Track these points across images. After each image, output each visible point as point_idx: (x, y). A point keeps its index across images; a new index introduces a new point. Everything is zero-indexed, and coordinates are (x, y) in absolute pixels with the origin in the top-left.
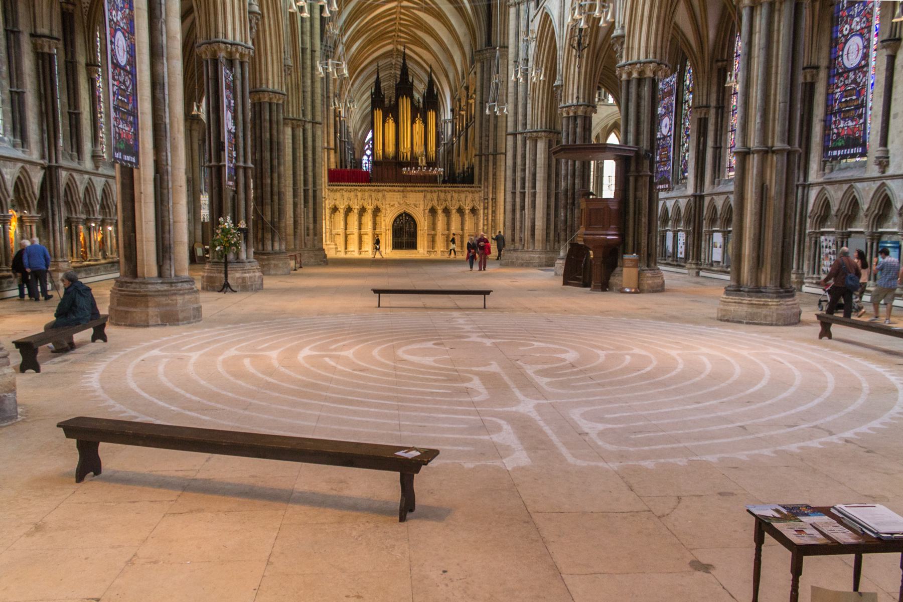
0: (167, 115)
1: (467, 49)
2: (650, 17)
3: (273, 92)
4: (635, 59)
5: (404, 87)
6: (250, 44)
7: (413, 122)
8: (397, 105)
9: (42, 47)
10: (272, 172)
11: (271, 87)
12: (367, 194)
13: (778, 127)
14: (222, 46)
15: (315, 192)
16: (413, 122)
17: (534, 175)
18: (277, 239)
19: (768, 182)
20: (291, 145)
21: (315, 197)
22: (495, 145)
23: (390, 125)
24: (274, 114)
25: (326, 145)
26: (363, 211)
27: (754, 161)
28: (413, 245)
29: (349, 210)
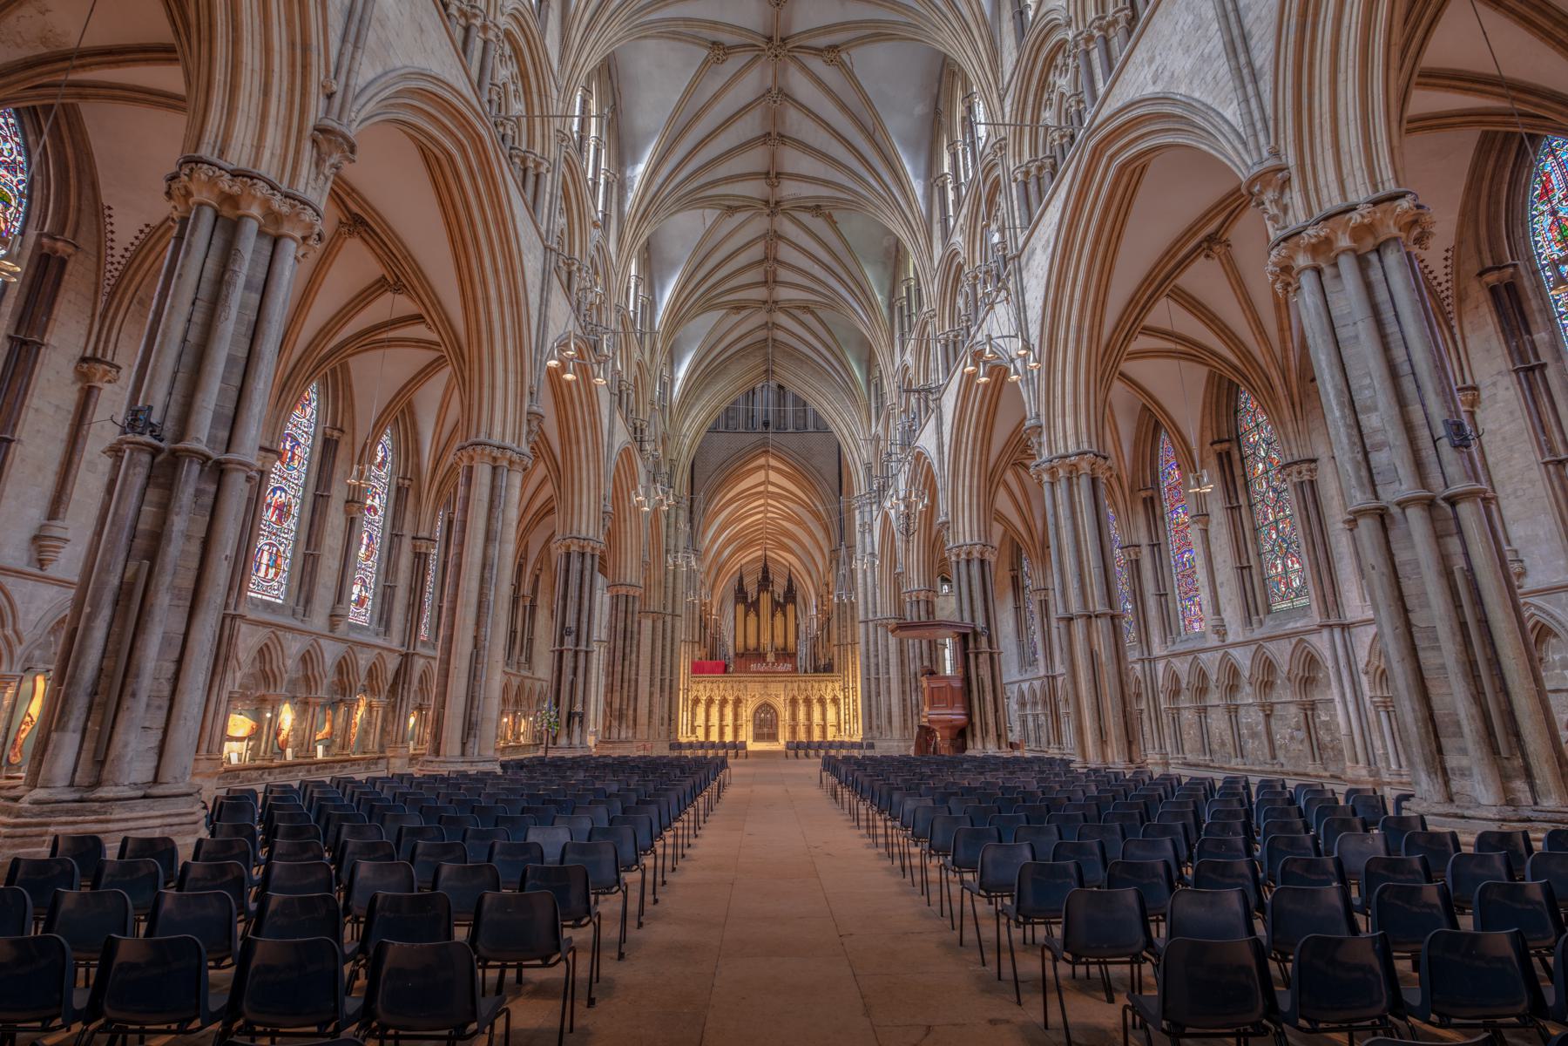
0: (493, 593)
1: (826, 551)
2: (970, 505)
4: (961, 541)
5: (765, 582)
6: (602, 538)
7: (773, 616)
8: (758, 598)
9: (420, 547)
11: (628, 581)
12: (729, 685)
14: (575, 541)
15: (671, 681)
16: (773, 616)
17: (888, 660)
18: (624, 726)
19: (1096, 648)
21: (671, 687)
22: (853, 635)
23: (752, 617)
24: (630, 605)
26: (724, 702)
27: (1078, 627)
28: (773, 737)
29: (710, 702)
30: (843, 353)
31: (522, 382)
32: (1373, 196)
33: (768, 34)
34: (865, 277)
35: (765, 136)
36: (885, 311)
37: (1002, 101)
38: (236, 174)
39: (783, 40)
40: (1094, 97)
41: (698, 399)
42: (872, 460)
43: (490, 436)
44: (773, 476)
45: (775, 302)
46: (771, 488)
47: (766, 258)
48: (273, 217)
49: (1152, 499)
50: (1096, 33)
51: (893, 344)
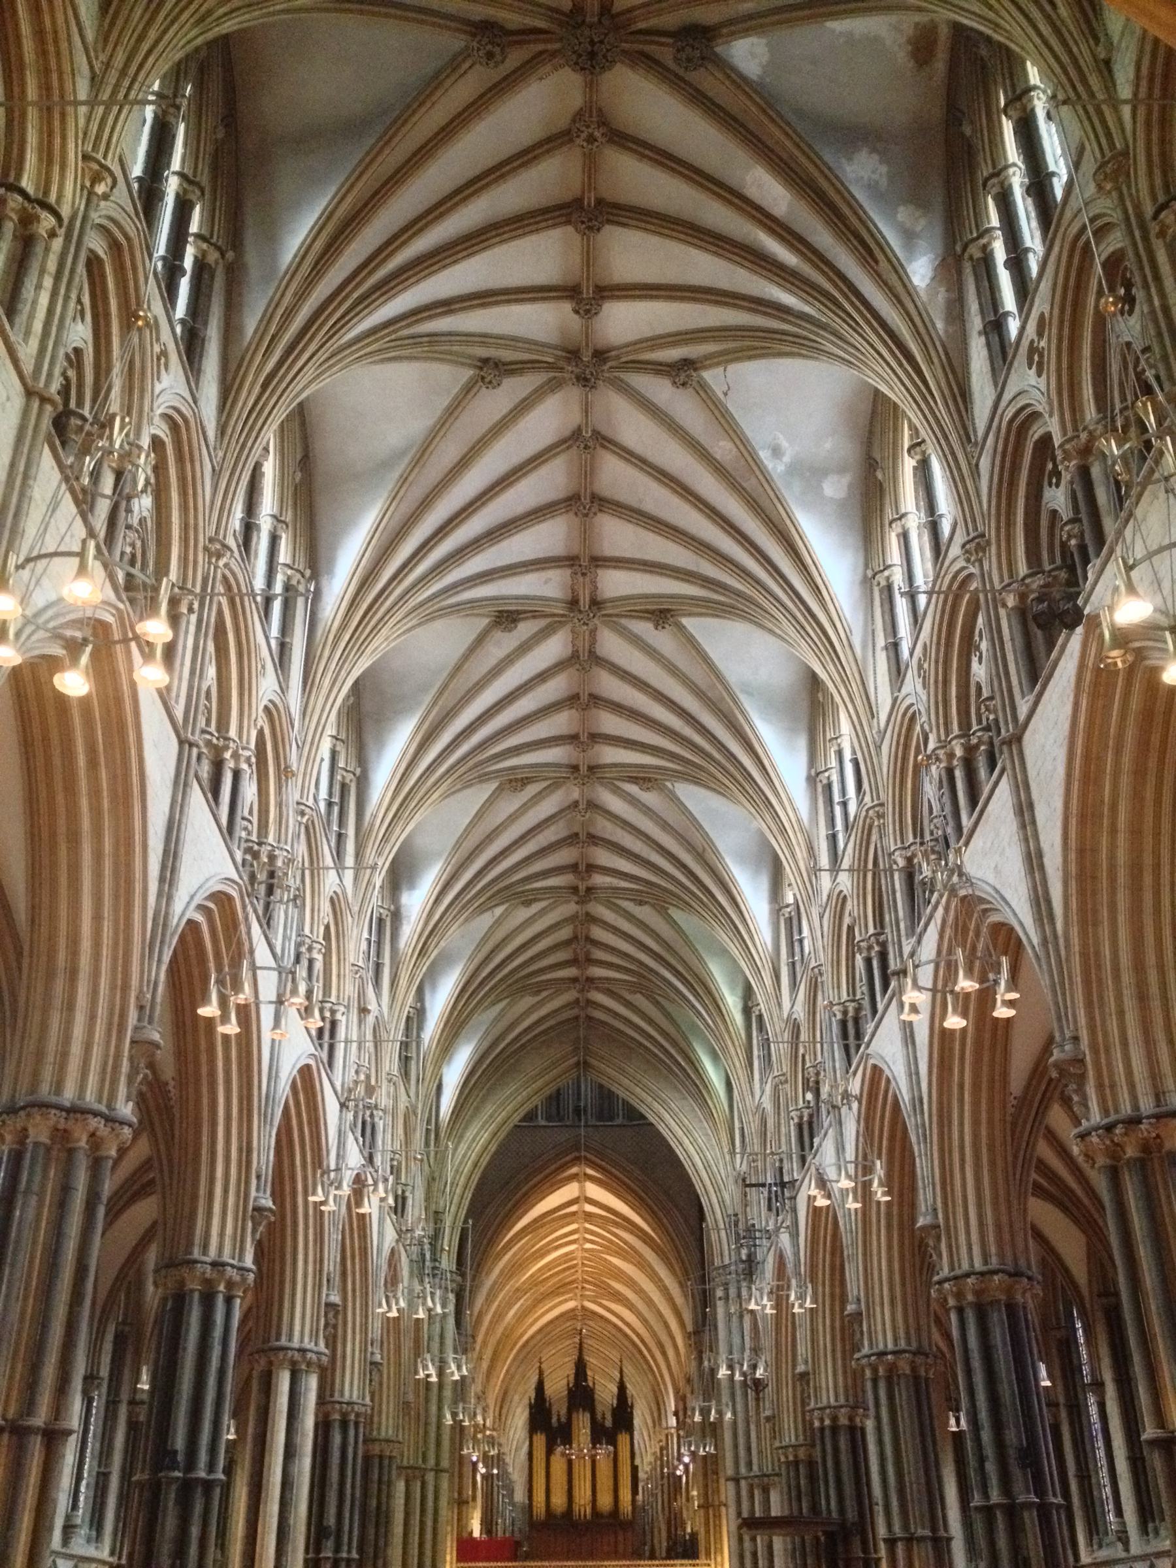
2: (833, 1351)
3: (388, 1441)
6: (368, 1399)
10: (376, 1557)
11: (383, 1434)
13: (915, 1511)
14: (337, 1406)
20: (402, 1508)
25: (456, 1495)
30: (690, 1045)
31: (321, 1271)
32: (985, 1268)
33: (574, 762)
34: (710, 974)
35: (570, 837)
36: (738, 1018)
37: (821, 917)
38: (214, 1264)
39: (591, 768)
40: (874, 1011)
41: (477, 1110)
42: (739, 1210)
43: (290, 1339)
44: (594, 1191)
45: (590, 980)
46: (589, 1208)
47: (575, 938)
48: (230, 1285)
49: (1067, 1341)
50: (877, 948)
51: (751, 1065)
